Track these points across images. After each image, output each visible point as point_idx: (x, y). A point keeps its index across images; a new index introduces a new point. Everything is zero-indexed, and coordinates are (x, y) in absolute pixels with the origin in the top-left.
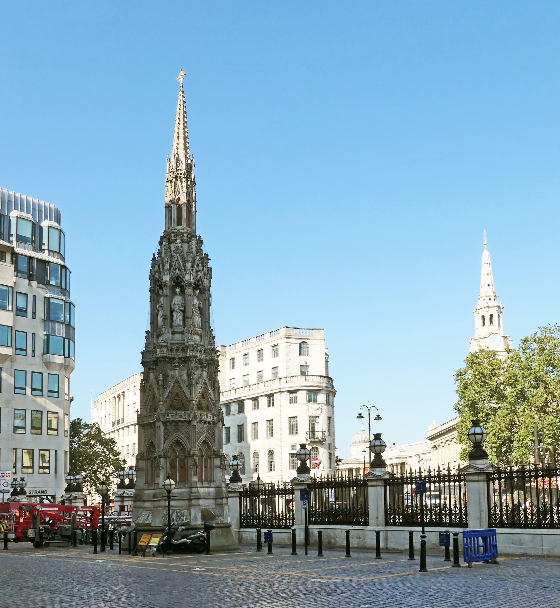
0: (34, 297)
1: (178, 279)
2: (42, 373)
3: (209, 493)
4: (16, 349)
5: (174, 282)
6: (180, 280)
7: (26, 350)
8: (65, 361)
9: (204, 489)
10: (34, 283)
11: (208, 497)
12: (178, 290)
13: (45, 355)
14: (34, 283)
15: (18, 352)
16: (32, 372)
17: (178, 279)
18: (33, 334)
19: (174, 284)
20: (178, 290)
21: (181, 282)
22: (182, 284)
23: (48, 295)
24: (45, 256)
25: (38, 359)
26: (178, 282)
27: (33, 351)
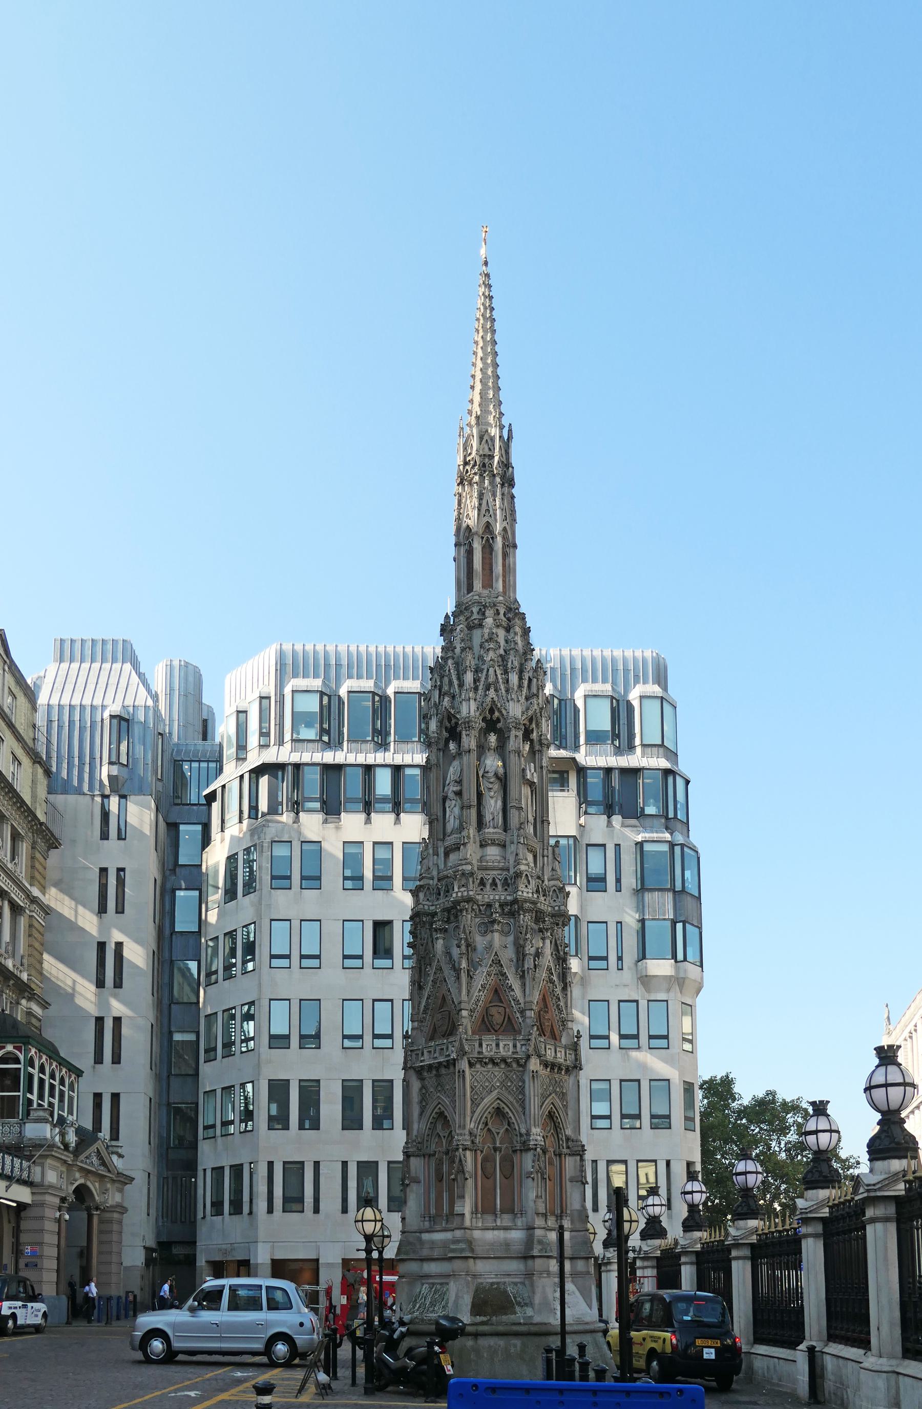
0: (618, 846)
1: (492, 711)
2: (637, 1001)
3: (507, 1244)
4: (591, 958)
5: (484, 719)
6: (497, 714)
7: (605, 958)
8: (677, 969)
9: (496, 1232)
10: (617, 820)
11: (503, 1253)
12: (493, 738)
13: (640, 963)
14: (617, 820)
15: (594, 964)
16: (620, 1001)
17: (492, 711)
18: (618, 922)
19: (484, 725)
20: (493, 738)
21: (498, 720)
22: (499, 725)
23: (639, 838)
24: (635, 760)
25: (627, 975)
26: (493, 723)
27: (620, 958)
